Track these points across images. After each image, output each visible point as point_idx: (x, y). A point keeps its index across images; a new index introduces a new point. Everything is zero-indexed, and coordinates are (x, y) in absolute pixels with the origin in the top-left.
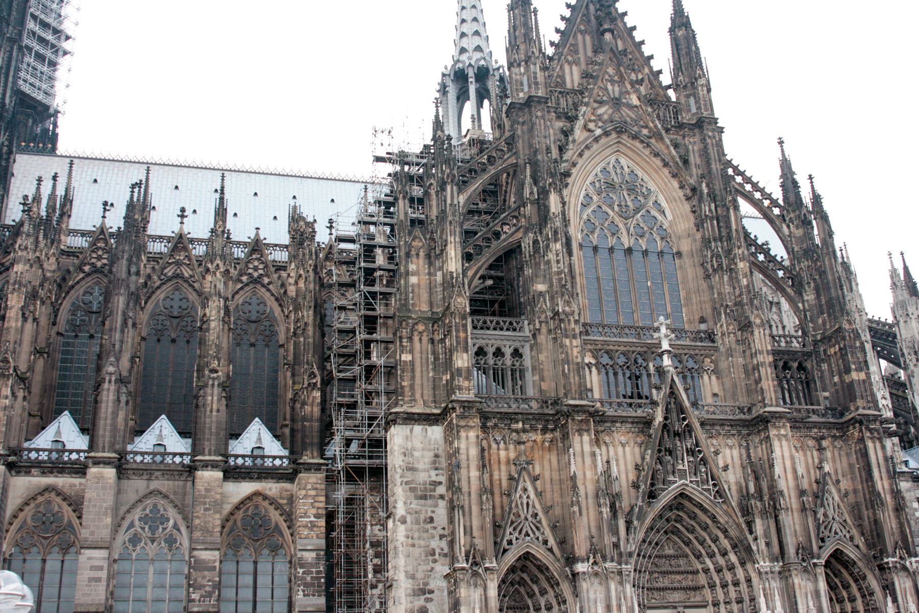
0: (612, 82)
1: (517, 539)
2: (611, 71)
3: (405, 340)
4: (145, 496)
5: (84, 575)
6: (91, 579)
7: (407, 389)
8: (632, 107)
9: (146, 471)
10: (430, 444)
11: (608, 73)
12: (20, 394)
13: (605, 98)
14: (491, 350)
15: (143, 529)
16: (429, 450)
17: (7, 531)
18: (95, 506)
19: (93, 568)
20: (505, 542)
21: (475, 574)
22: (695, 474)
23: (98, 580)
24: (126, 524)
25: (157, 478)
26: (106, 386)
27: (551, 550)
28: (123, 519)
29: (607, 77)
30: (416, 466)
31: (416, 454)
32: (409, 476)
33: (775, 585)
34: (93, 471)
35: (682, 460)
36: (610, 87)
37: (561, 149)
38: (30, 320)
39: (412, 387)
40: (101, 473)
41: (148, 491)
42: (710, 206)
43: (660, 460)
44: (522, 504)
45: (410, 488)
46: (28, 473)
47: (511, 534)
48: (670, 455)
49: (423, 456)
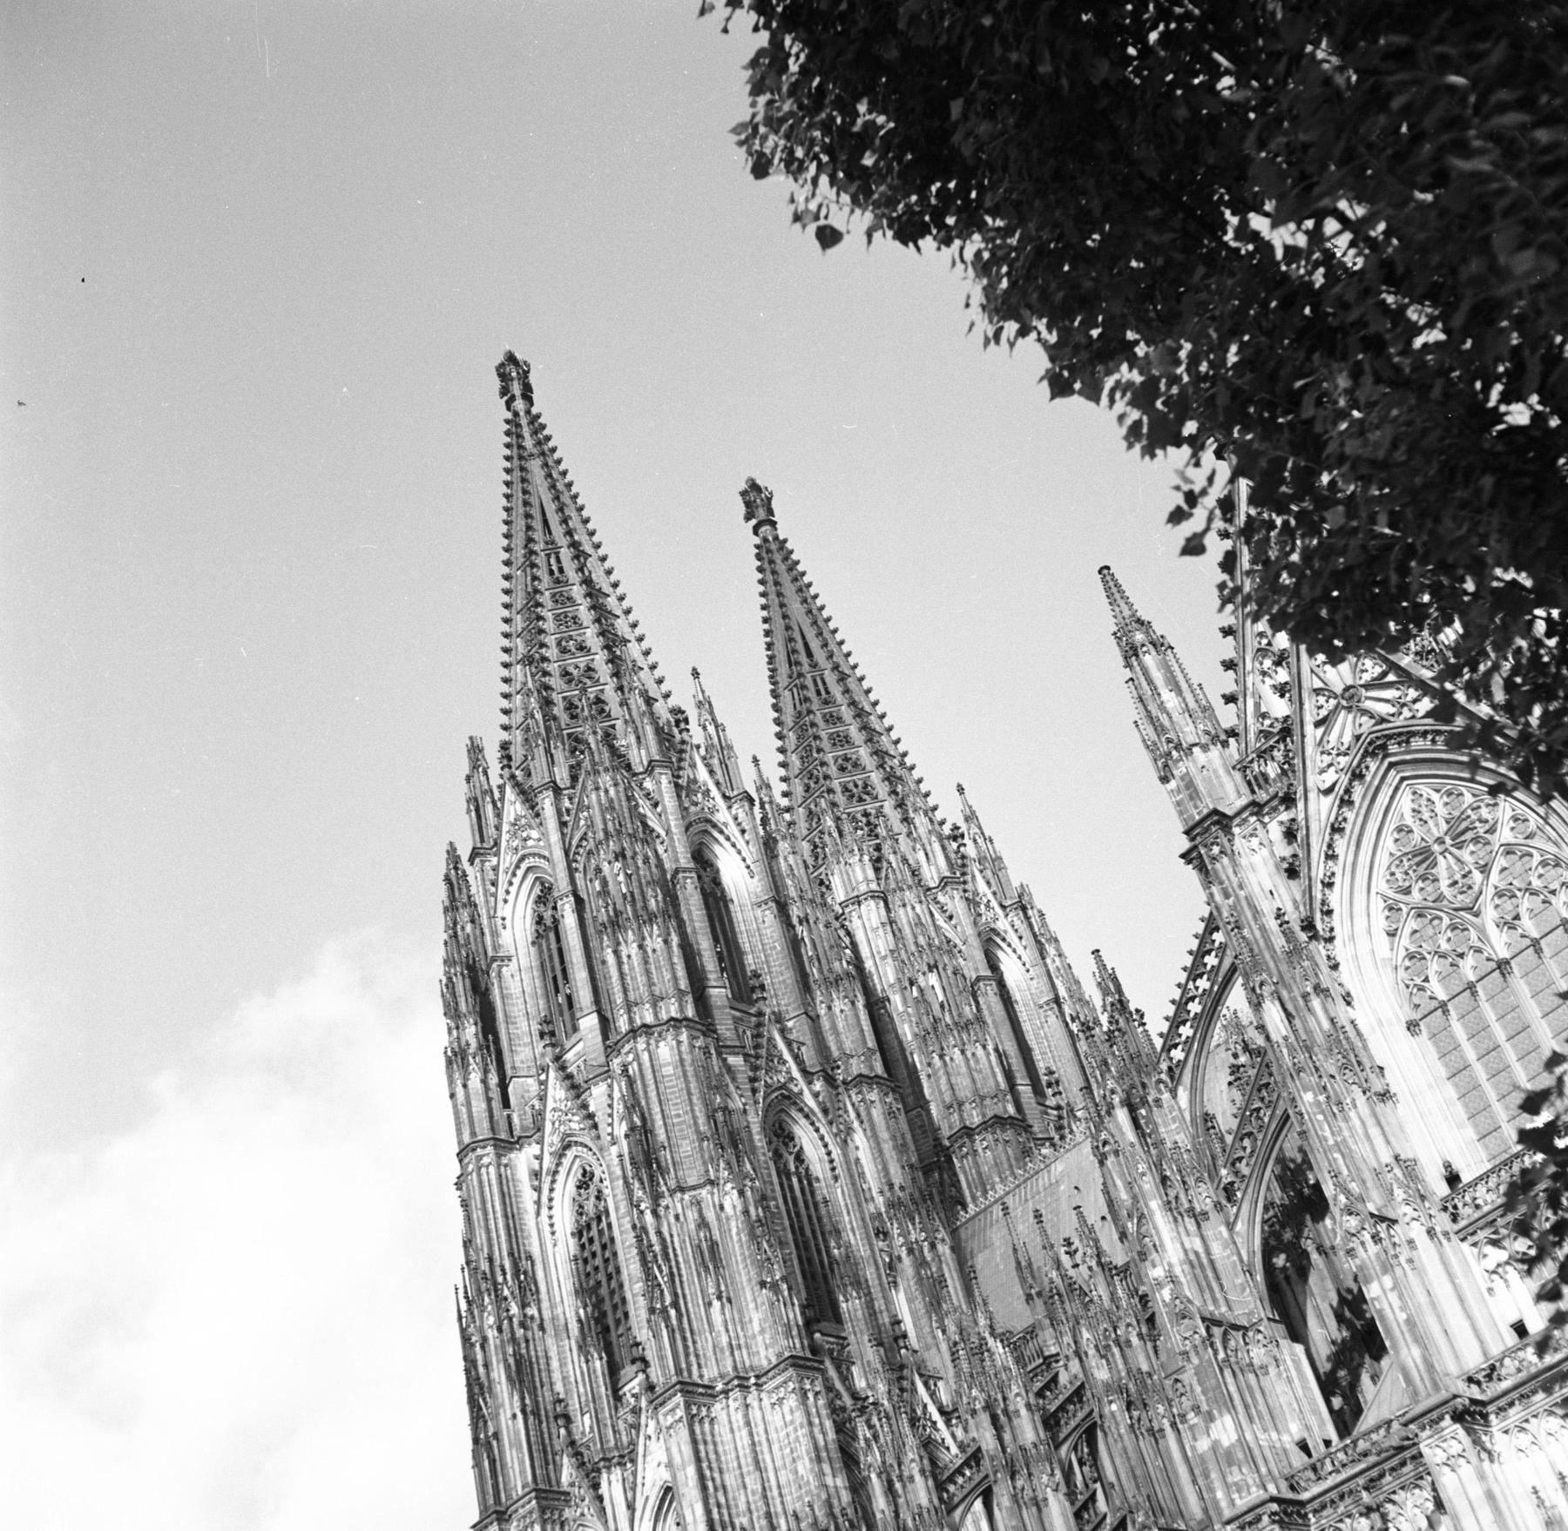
37: (1292, 873)
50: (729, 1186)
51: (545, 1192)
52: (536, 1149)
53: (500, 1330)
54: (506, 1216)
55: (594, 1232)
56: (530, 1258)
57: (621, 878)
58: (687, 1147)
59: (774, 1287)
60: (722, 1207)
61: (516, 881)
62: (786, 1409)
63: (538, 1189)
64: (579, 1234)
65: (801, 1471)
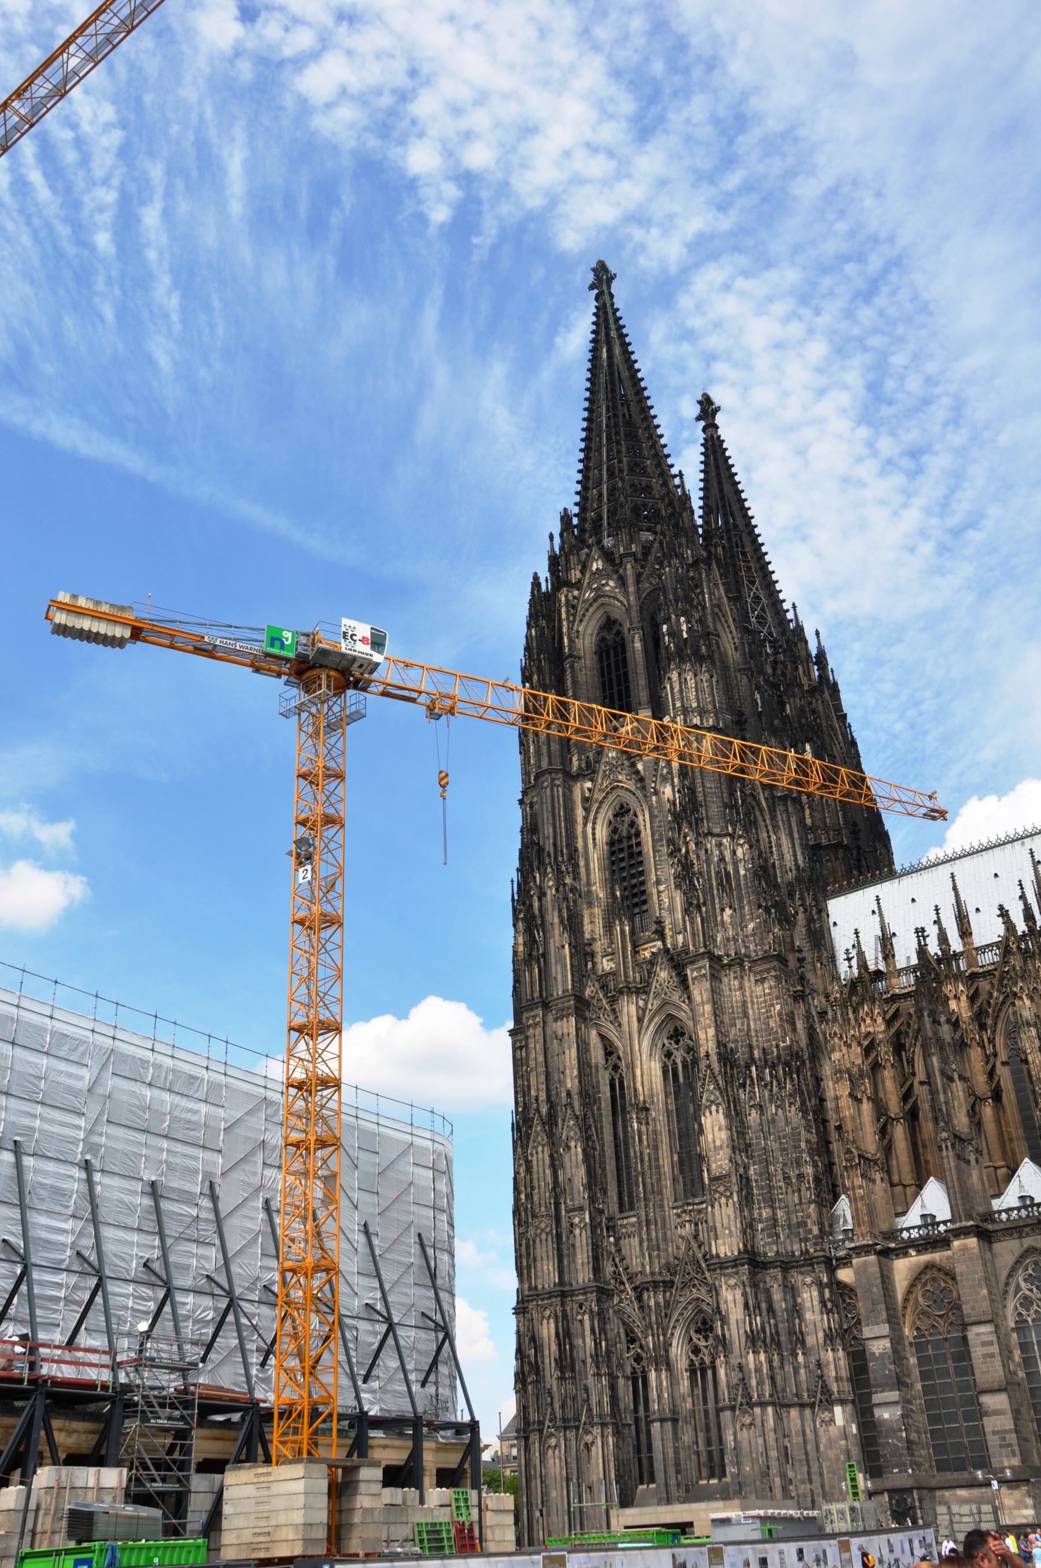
4: (1023, 1256)
5: (977, 1352)
6: (985, 1356)
9: (1015, 1230)
12: (878, 1177)
15: (1031, 1290)
17: (904, 1316)
18: (967, 1280)
19: (984, 1344)
23: (992, 1355)
24: (1012, 1289)
25: (1028, 1235)
26: (944, 1153)
28: (1007, 1284)
34: (956, 1243)
38: (865, 1100)
40: (965, 1245)
41: (1022, 1250)
46: (906, 1255)
50: (741, 841)
51: (592, 814)
52: (589, 785)
53: (557, 890)
54: (566, 820)
55: (625, 845)
56: (576, 850)
57: (684, 627)
58: (714, 809)
59: (767, 910)
60: (734, 852)
61: (591, 610)
62: (766, 985)
63: (587, 810)
64: (611, 843)
65: (772, 1024)
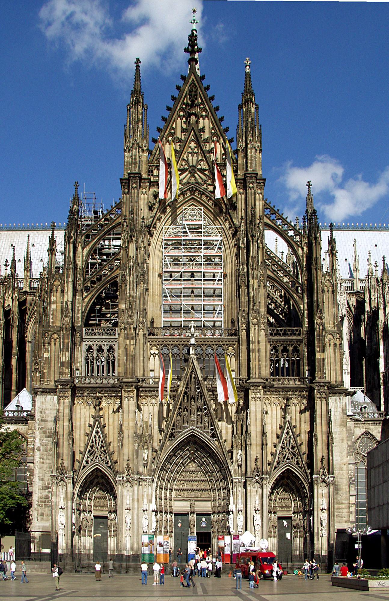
0: (192, 153)
1: (92, 460)
2: (193, 145)
3: (47, 345)
7: (46, 374)
8: (202, 171)
10: (55, 406)
11: (190, 147)
13: (186, 167)
14: (95, 348)
16: (54, 410)
20: (84, 462)
21: (62, 480)
22: (201, 423)
27: (110, 467)
29: (190, 150)
30: (47, 419)
31: (47, 412)
32: (43, 425)
33: (240, 489)
35: (194, 414)
36: (190, 157)
39: (49, 373)
42: (243, 240)
43: (179, 414)
44: (96, 441)
45: (43, 431)
47: (88, 457)
48: (187, 411)
49: (51, 414)
